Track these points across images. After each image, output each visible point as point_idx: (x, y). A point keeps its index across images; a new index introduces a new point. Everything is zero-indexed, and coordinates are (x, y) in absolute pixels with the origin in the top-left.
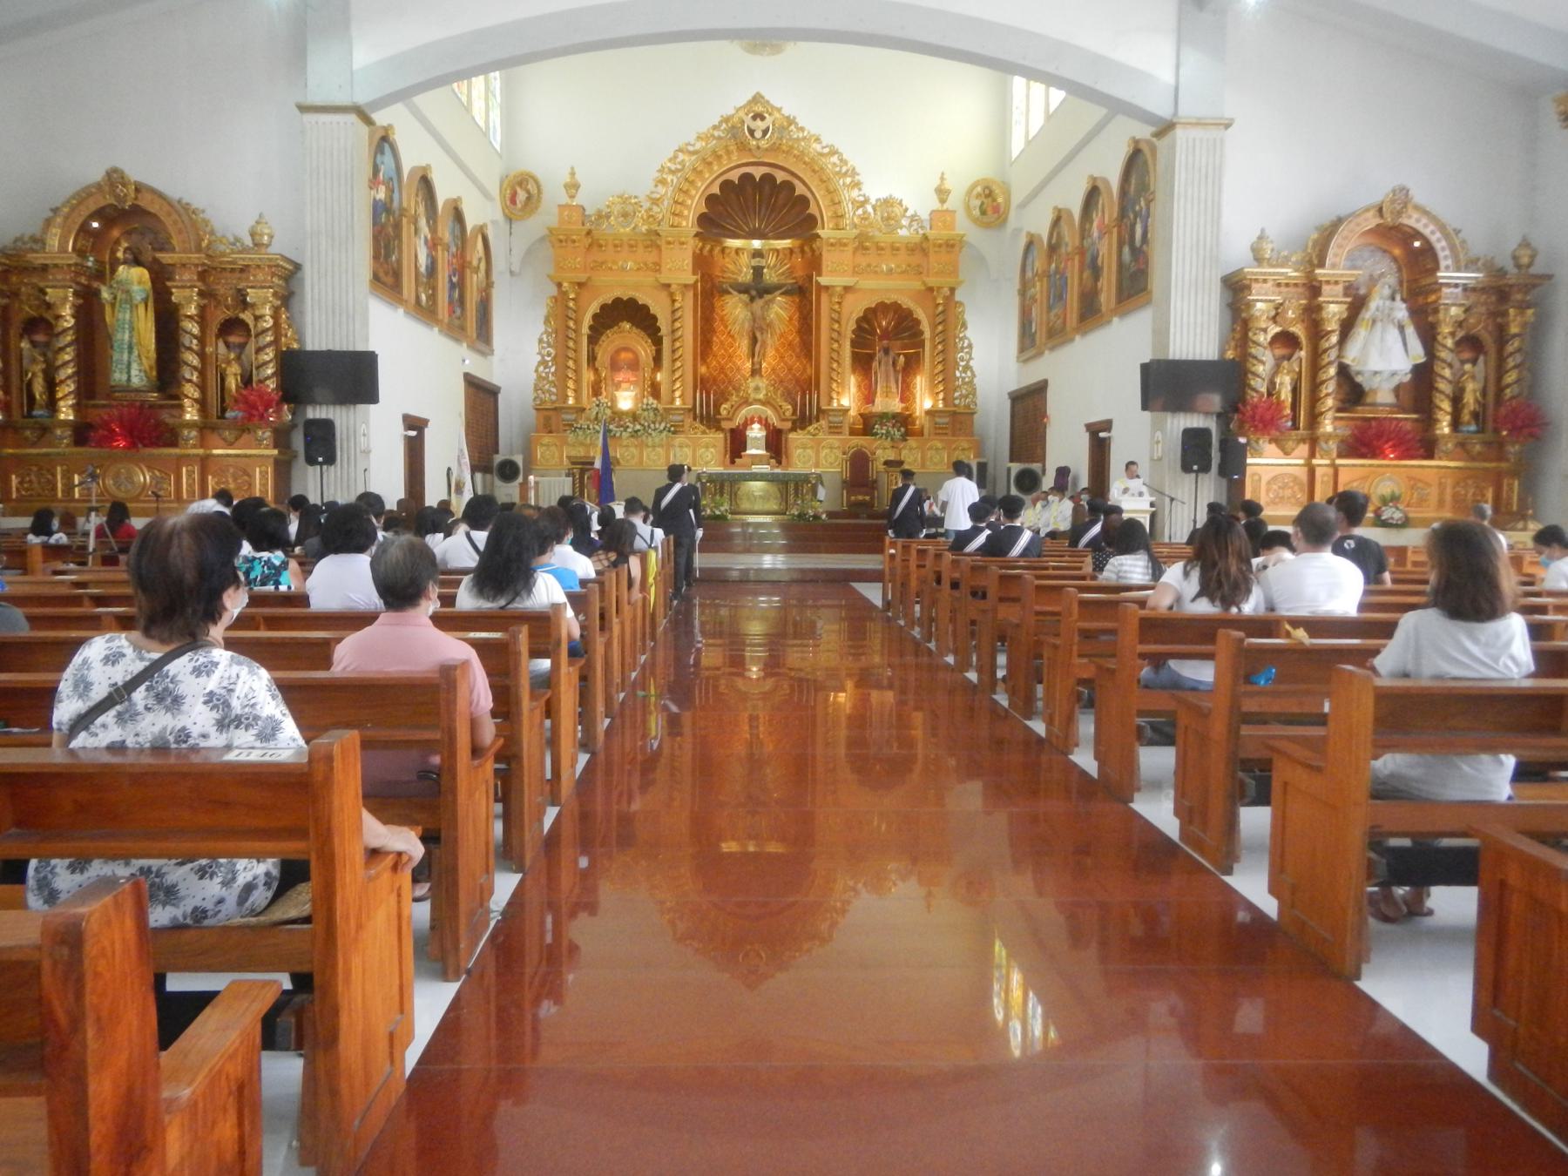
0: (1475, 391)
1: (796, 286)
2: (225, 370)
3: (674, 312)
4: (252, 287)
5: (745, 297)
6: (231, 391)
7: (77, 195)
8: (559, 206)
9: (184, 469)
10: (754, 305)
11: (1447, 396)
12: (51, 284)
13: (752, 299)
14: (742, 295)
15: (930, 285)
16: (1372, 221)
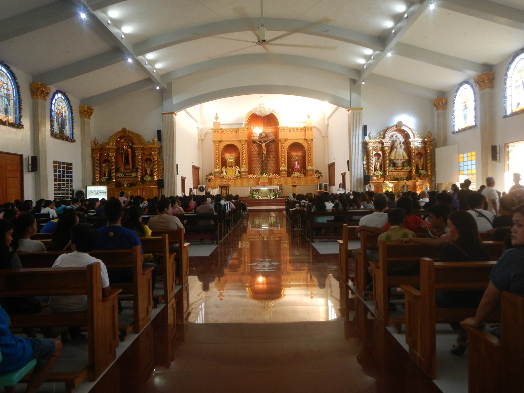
0: (421, 165)
1: (273, 140)
2: (147, 169)
4: (153, 152)
6: (148, 174)
7: (115, 134)
8: (214, 123)
9: (138, 191)
11: (414, 166)
12: (110, 152)
13: (262, 143)
15: (306, 139)
16: (395, 128)
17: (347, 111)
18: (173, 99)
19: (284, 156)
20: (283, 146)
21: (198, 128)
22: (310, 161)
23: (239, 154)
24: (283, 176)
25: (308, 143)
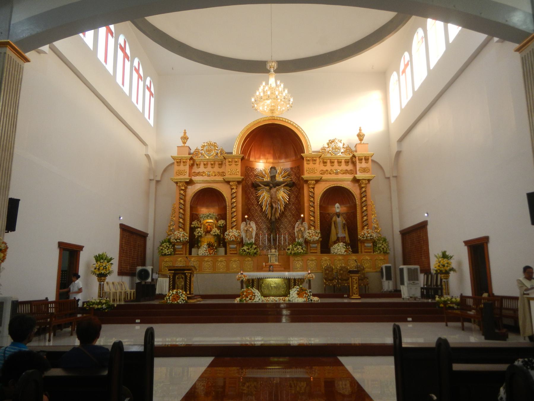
1: (291, 182)
3: (232, 194)
5: (268, 188)
8: (178, 147)
10: (272, 191)
13: (271, 188)
14: (266, 187)
15: (357, 178)
17: (518, 50)
18: (15, 9)
19: (314, 213)
20: (311, 192)
21: (147, 156)
22: (365, 224)
23: (225, 208)
24: (312, 252)
25: (363, 187)
